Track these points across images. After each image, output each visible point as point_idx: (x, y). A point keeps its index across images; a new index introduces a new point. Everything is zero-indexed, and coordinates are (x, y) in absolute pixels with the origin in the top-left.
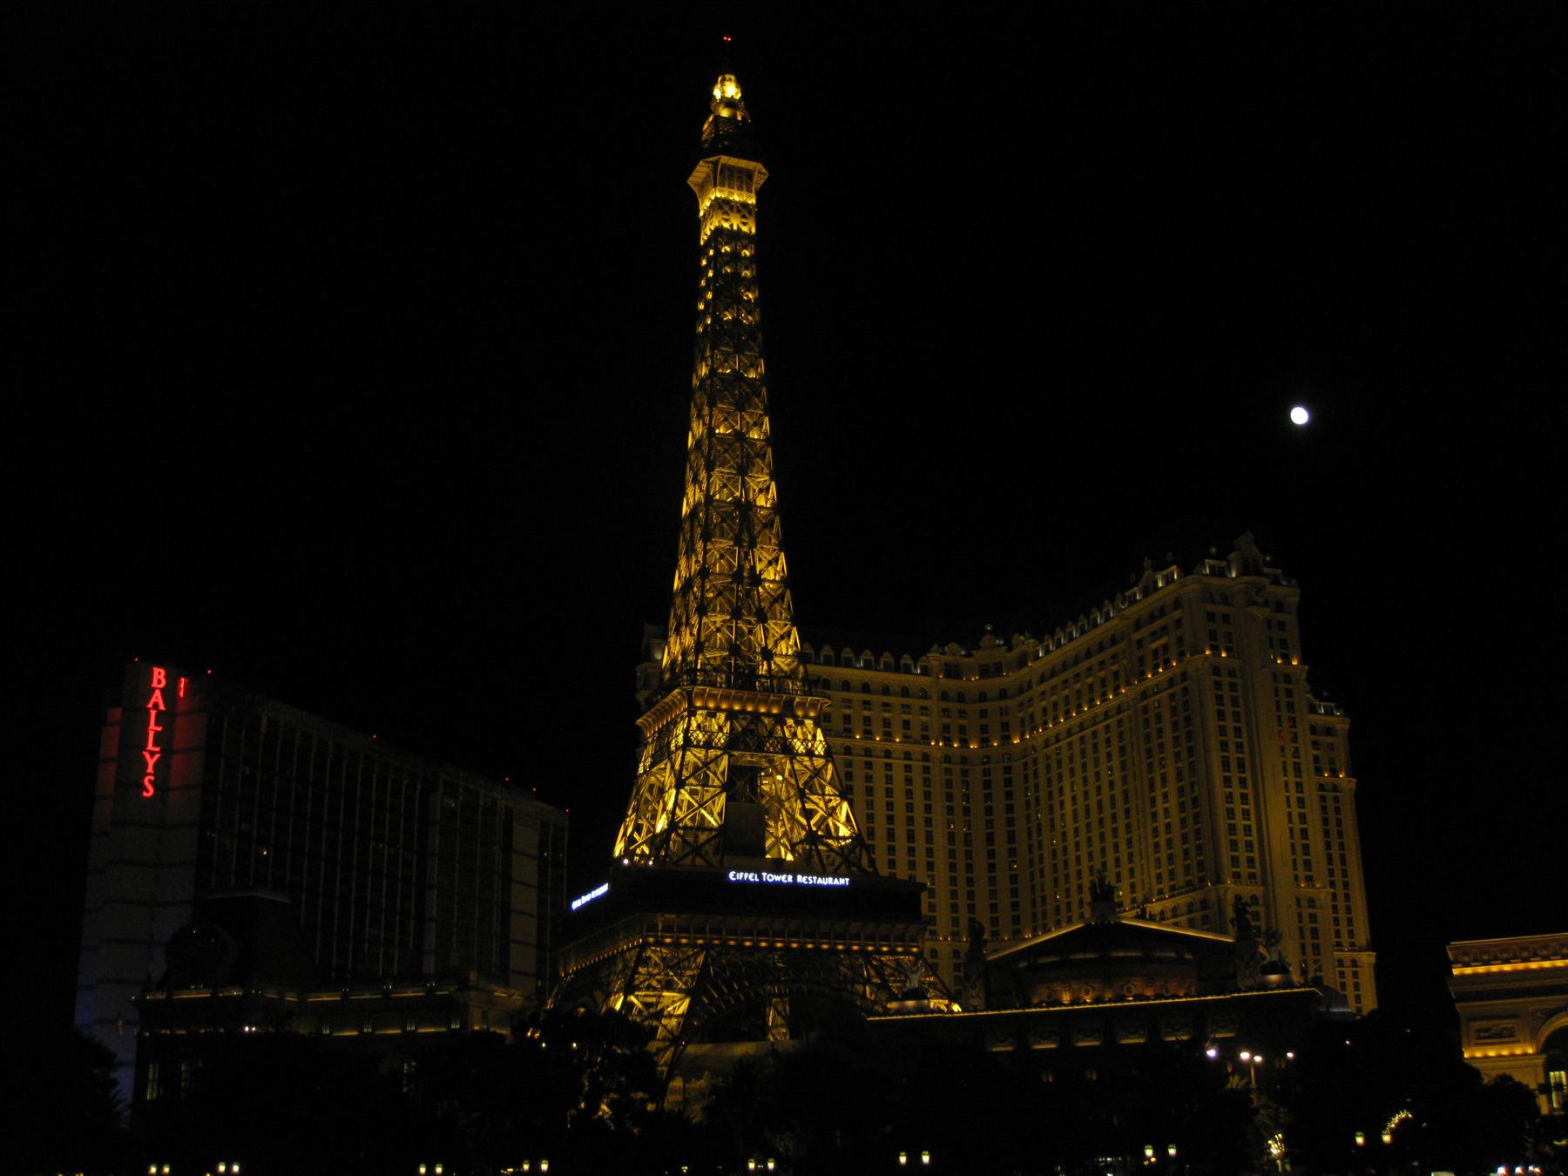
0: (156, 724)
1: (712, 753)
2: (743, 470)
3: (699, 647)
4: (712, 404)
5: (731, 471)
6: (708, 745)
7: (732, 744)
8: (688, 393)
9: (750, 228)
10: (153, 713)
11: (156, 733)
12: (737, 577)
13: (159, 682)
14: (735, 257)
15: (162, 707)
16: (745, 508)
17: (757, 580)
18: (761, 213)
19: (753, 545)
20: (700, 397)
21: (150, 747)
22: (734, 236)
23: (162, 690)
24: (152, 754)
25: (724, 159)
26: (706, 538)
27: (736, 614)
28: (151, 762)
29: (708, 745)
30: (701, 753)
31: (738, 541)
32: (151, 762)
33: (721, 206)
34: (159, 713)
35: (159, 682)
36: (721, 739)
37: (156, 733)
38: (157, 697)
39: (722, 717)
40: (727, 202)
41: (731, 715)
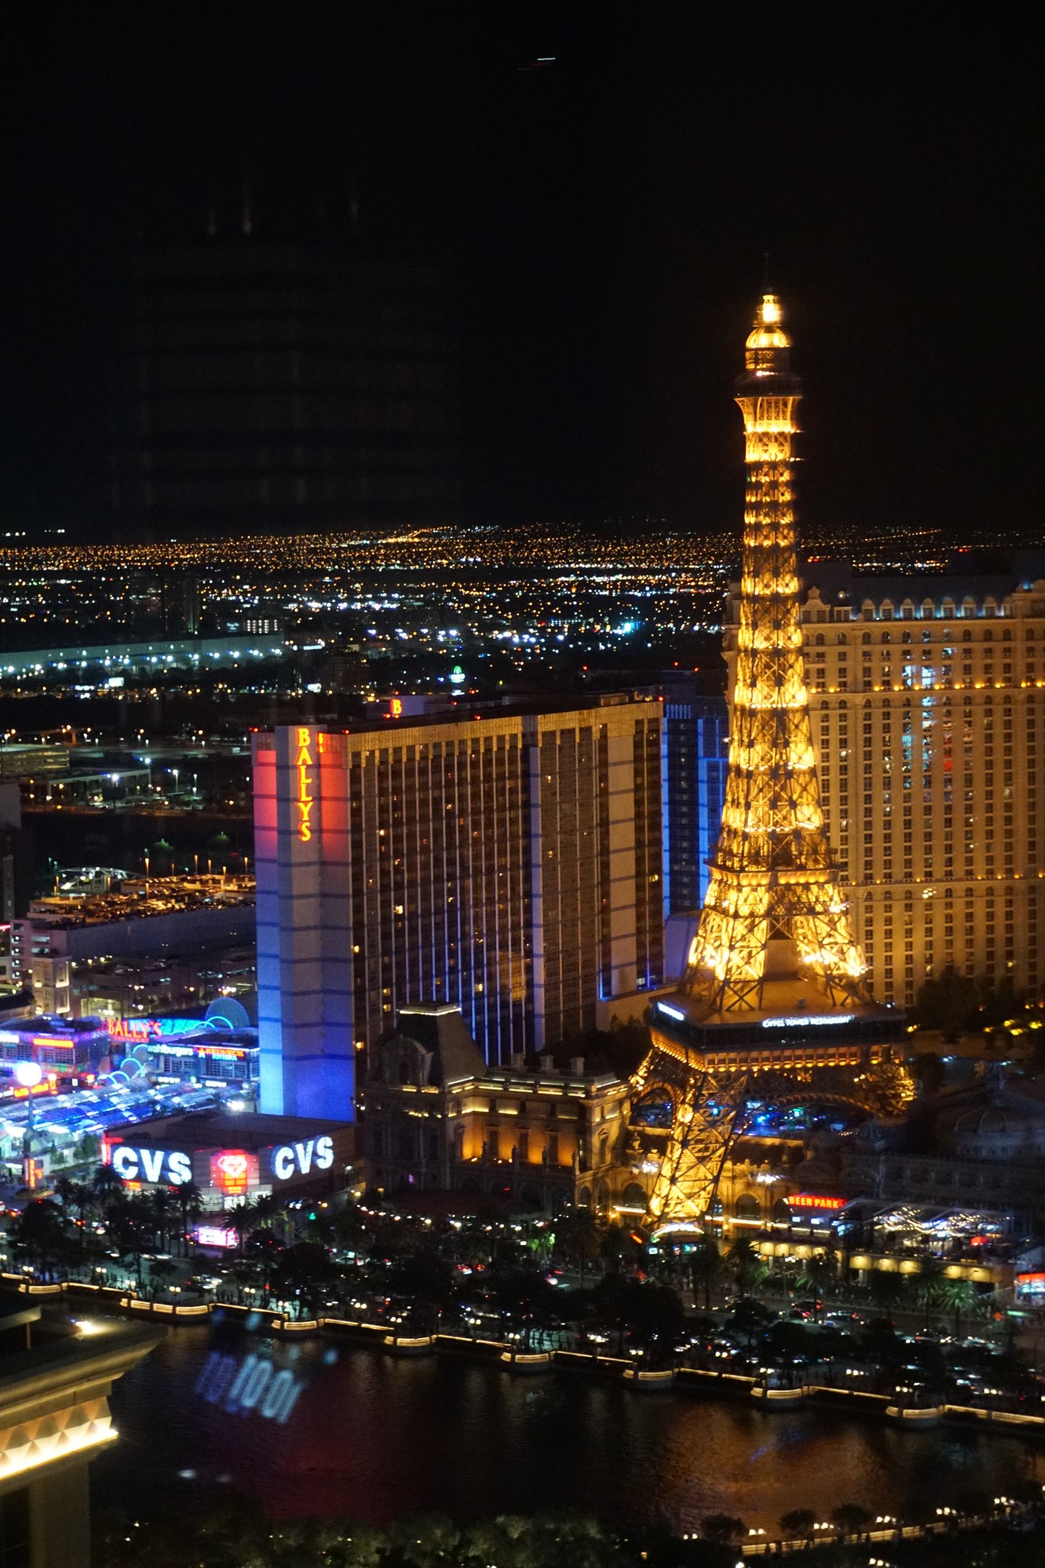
0: (307, 777)
10: (303, 769)
11: (308, 785)
13: (305, 740)
14: (774, 485)
15: (309, 762)
18: (797, 442)
19: (787, 744)
21: (304, 798)
22: (773, 465)
23: (307, 747)
24: (306, 803)
27: (774, 805)
28: (305, 810)
32: (305, 810)
33: (763, 438)
34: (308, 767)
35: (305, 740)
37: (308, 785)
38: (305, 756)
40: (766, 434)
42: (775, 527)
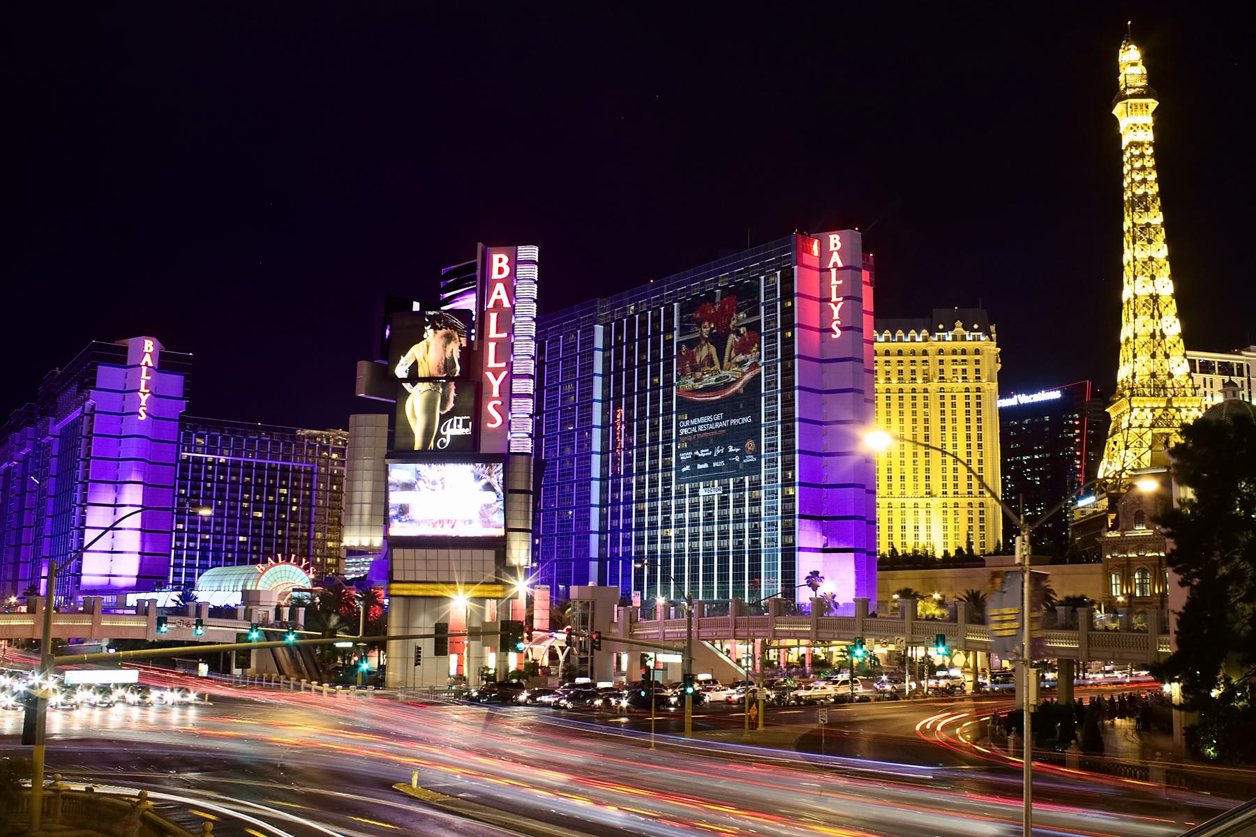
1: (1143, 430)
2: (1153, 277)
3: (1134, 376)
4: (1133, 211)
5: (1147, 274)
6: (1141, 426)
7: (1152, 426)
8: (1121, 234)
9: (1150, 137)
12: (1153, 336)
14: (1142, 156)
16: (1155, 298)
17: (1163, 336)
20: (1128, 238)
25: (1131, 101)
26: (1135, 316)
27: (1153, 356)
29: (1141, 426)
30: (1137, 430)
31: (1152, 316)
36: (1147, 423)
39: (1147, 411)
41: (1153, 410)
42: (1144, 181)
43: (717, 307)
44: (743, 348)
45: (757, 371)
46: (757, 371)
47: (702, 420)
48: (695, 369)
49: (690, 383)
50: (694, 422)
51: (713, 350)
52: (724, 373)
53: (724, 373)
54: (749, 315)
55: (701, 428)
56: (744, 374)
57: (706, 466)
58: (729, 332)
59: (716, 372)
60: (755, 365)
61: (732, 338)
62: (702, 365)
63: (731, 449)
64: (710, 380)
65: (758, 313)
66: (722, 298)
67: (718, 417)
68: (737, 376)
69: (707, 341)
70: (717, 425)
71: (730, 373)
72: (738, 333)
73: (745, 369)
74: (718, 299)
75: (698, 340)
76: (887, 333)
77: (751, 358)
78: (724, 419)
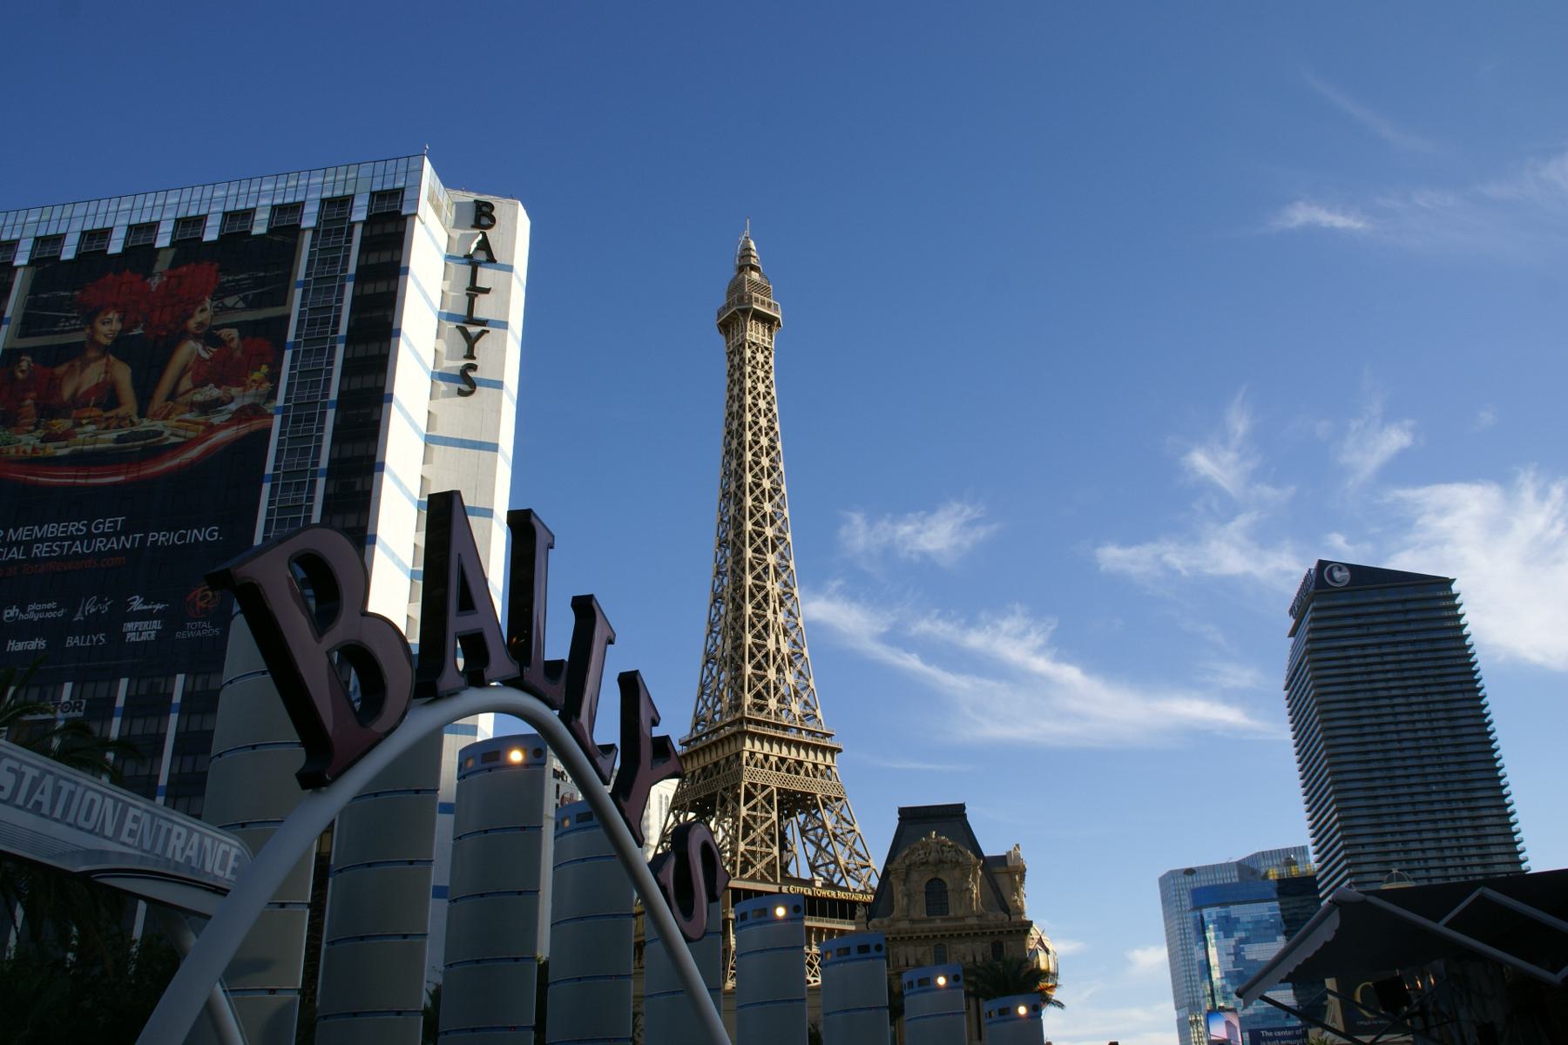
43: (155, 282)
44: (225, 371)
45: (257, 424)
46: (257, 424)
47: (51, 529)
48: (48, 411)
49: (28, 442)
50: (22, 533)
51: (123, 374)
52: (146, 425)
53: (146, 425)
54: (251, 305)
55: (40, 550)
56: (211, 429)
57: (38, 644)
58: (182, 335)
59: (121, 422)
60: (254, 411)
61: (189, 350)
62: (78, 402)
63: (137, 604)
64: (95, 436)
65: (282, 299)
66: (174, 265)
67: (107, 526)
68: (187, 428)
69: (105, 350)
70: (99, 544)
71: (167, 429)
72: (209, 337)
73: (216, 420)
74: (162, 265)
75: (73, 354)
76: (301, 574)
77: (241, 398)
78: (127, 531)
